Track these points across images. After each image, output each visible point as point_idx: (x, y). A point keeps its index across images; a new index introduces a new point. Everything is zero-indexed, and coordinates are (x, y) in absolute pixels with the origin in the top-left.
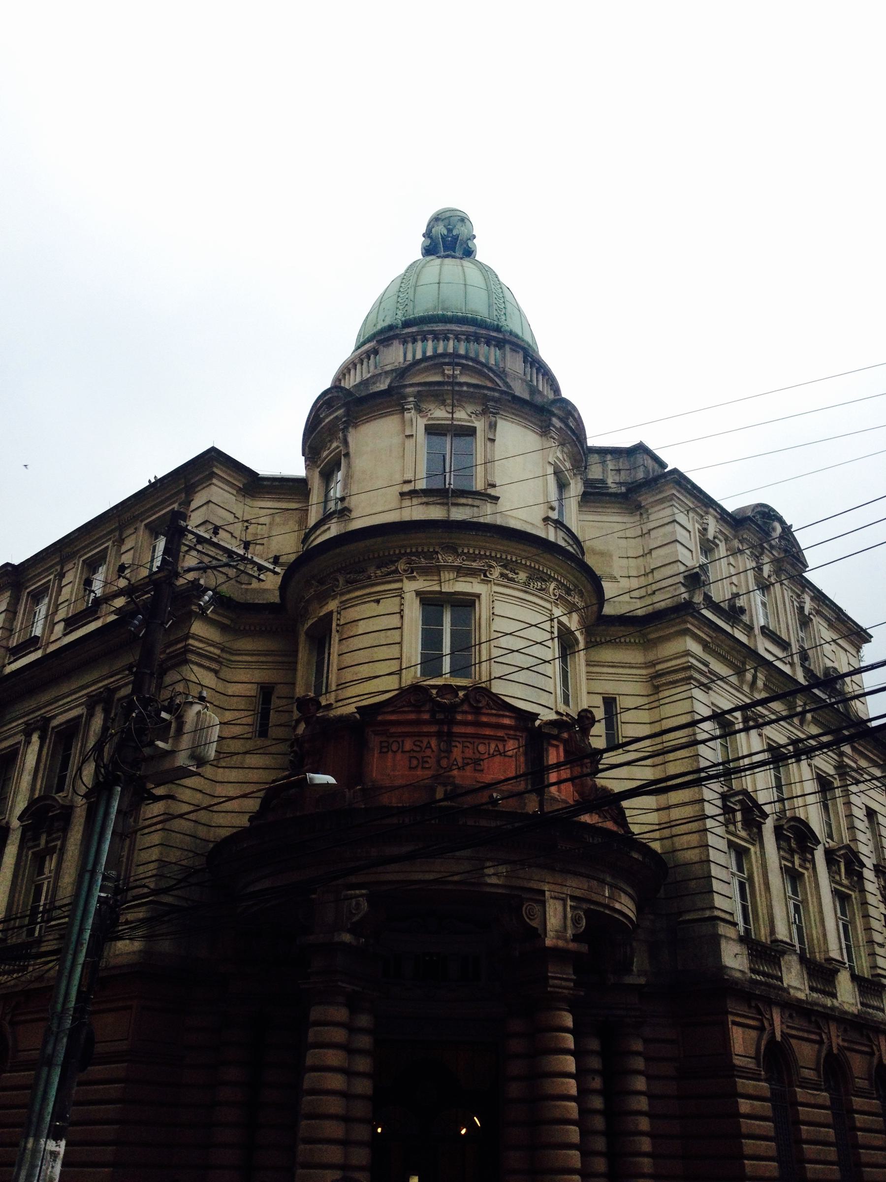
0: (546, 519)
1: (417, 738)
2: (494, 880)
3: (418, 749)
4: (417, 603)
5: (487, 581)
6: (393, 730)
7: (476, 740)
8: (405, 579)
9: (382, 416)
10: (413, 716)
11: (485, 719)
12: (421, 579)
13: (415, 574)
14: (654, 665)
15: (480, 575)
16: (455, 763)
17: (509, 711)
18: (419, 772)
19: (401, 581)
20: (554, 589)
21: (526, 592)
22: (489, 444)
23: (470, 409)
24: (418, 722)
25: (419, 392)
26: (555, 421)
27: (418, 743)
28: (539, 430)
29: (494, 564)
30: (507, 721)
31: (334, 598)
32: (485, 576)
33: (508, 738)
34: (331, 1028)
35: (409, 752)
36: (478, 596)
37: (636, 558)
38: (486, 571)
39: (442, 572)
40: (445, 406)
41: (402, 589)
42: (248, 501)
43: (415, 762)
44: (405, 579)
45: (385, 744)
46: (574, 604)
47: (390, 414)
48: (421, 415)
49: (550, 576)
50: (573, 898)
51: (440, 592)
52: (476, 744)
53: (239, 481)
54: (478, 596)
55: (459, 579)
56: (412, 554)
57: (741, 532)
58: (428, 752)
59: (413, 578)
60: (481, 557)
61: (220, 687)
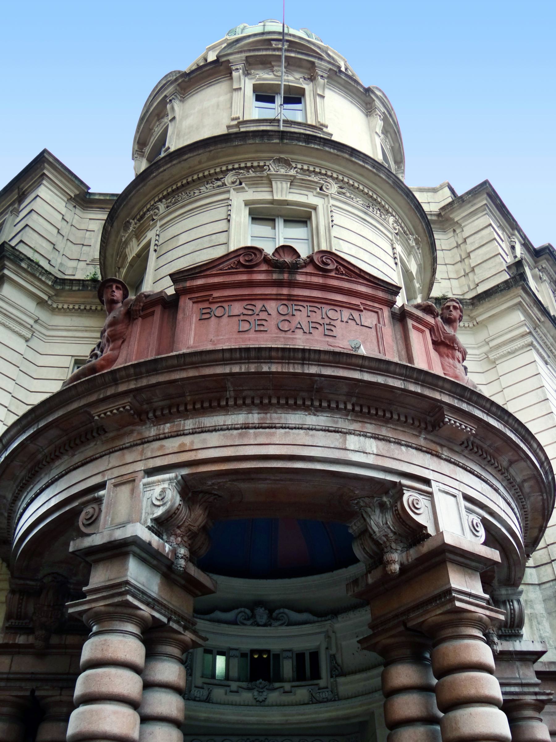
1: (249, 302)
3: (250, 312)
4: (245, 212)
6: (216, 294)
7: (323, 306)
8: (232, 191)
9: (210, 85)
10: (244, 277)
12: (250, 191)
13: (243, 185)
14: (488, 343)
15: (316, 189)
16: (299, 326)
18: (252, 335)
19: (229, 191)
20: (393, 224)
21: (366, 213)
22: (318, 99)
23: (298, 76)
25: (247, 57)
29: (330, 180)
31: (155, 225)
32: (321, 189)
33: (364, 309)
34: (112, 671)
35: (239, 315)
36: (315, 208)
37: (453, 265)
38: (323, 184)
39: (274, 183)
40: (273, 72)
41: (228, 199)
42: (78, 211)
44: (232, 191)
45: (204, 311)
47: (217, 82)
48: (250, 77)
50: (467, 498)
51: (273, 202)
52: (324, 310)
53: (72, 191)
54: (315, 208)
55: (292, 190)
56: (240, 168)
57: (541, 263)
58: (263, 315)
61: (30, 355)
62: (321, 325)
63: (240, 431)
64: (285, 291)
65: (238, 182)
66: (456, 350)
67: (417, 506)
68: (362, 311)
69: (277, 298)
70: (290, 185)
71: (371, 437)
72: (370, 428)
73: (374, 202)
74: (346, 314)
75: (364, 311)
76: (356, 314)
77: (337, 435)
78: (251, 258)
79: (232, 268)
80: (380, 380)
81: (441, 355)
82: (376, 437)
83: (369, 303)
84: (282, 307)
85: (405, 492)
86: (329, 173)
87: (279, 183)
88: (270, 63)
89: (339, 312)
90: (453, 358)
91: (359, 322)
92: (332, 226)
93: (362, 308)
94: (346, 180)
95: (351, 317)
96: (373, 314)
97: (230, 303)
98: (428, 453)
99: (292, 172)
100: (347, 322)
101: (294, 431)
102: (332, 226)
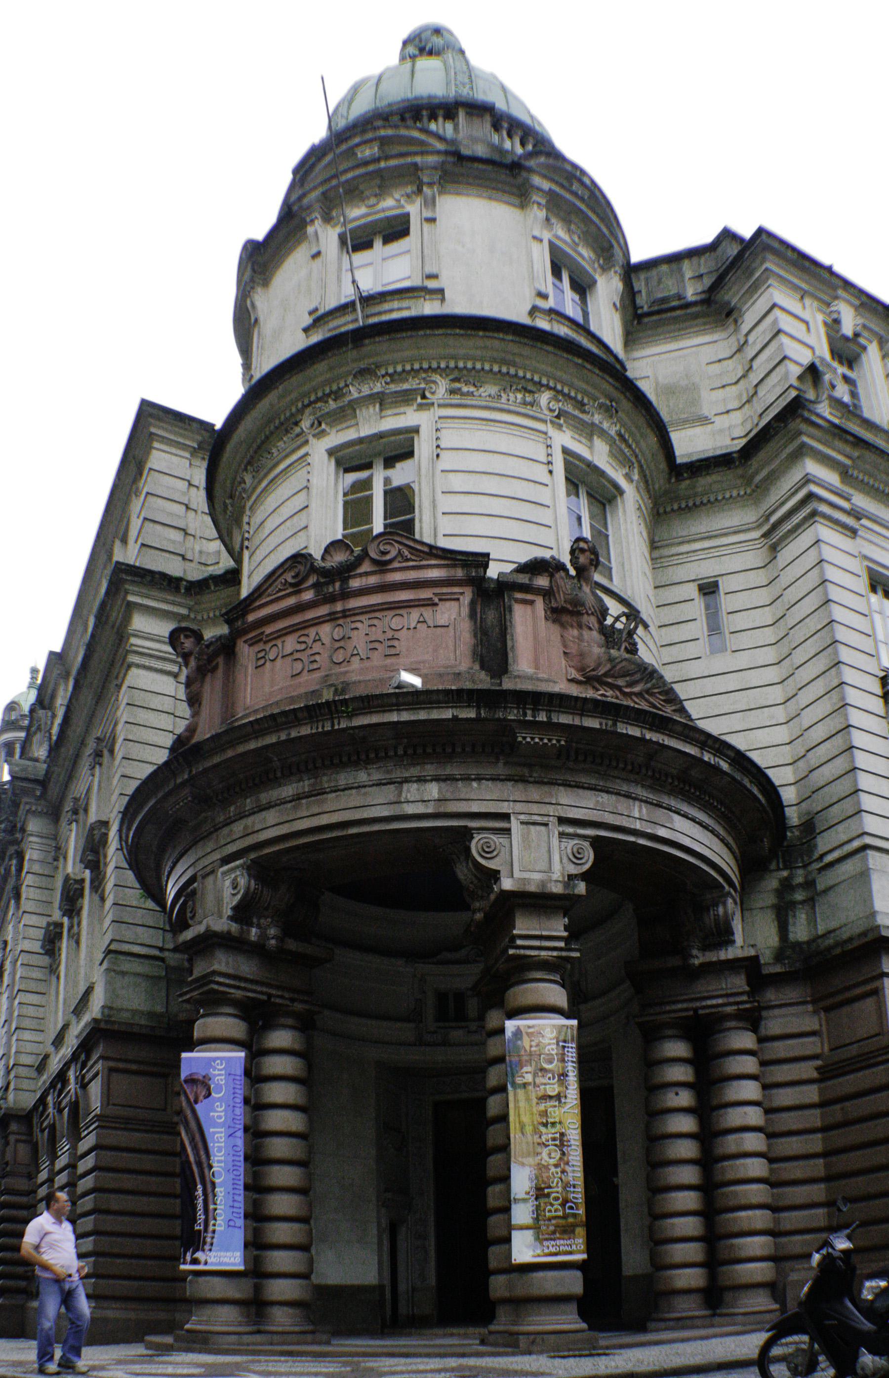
0: (534, 311)
2: (420, 809)
3: (303, 646)
5: (427, 404)
6: (269, 630)
7: (385, 613)
8: (310, 438)
10: (291, 601)
11: (398, 577)
13: (323, 426)
15: (416, 399)
17: (437, 557)
18: (305, 677)
24: (301, 608)
26: (537, 180)
27: (302, 639)
28: (517, 201)
29: (436, 377)
30: (434, 574)
32: (424, 397)
33: (440, 600)
35: (292, 654)
36: (416, 430)
38: (424, 390)
39: (358, 412)
43: (298, 666)
44: (310, 438)
46: (593, 424)
49: (540, 383)
51: (360, 441)
55: (383, 414)
56: (318, 400)
58: (317, 647)
59: (321, 434)
60: (414, 372)
62: (381, 642)
63: (293, 803)
64: (339, 607)
65: (316, 422)
66: (583, 614)
67: (487, 850)
68: (436, 605)
69: (332, 618)
70: (381, 405)
71: (431, 781)
72: (430, 770)
73: (515, 380)
74: (415, 614)
75: (441, 603)
76: (427, 613)
77: (392, 786)
78: (296, 570)
79: (280, 590)
80: (422, 715)
81: (563, 626)
82: (437, 779)
83: (445, 590)
84: (337, 629)
85: (475, 835)
86: (434, 365)
87: (364, 410)
88: (357, 188)
89: (405, 615)
90: (580, 626)
91: (431, 623)
92: (438, 456)
93: (436, 600)
94: (461, 364)
95: (421, 619)
96: (453, 603)
97: (283, 639)
98: (509, 780)
99: (378, 387)
100: (415, 628)
101: (346, 792)
102: (438, 456)
